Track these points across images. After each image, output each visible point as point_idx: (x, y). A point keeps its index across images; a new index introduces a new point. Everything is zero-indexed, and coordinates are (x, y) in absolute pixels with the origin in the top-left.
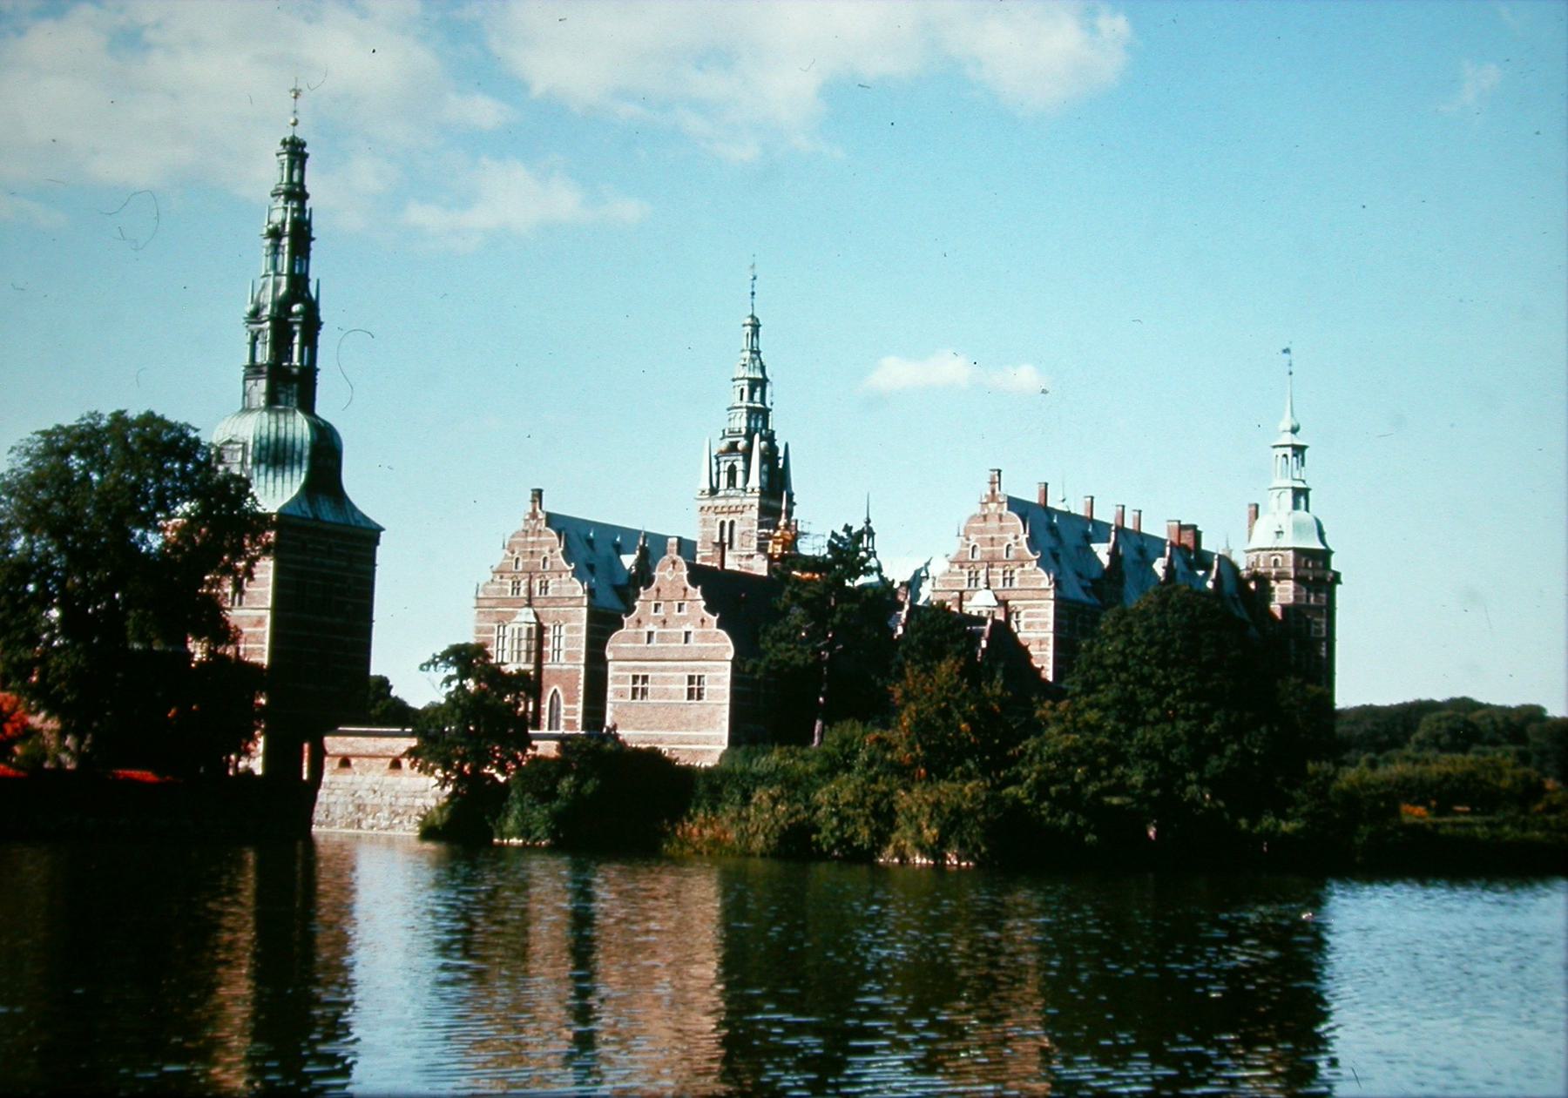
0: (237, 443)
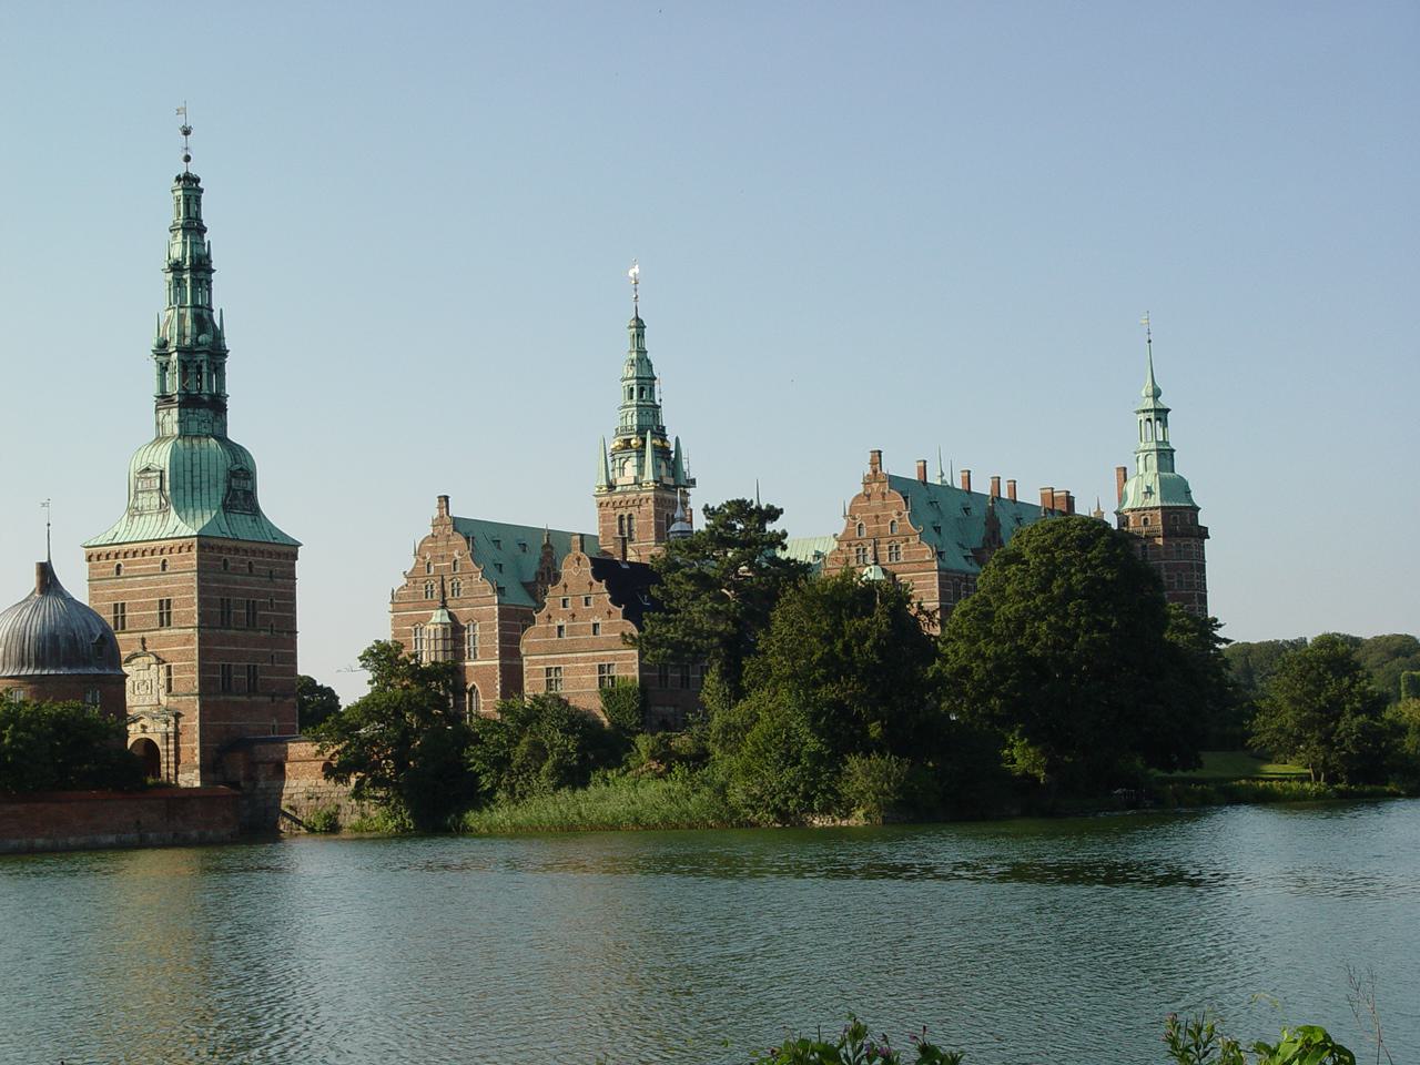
0: (155, 471)
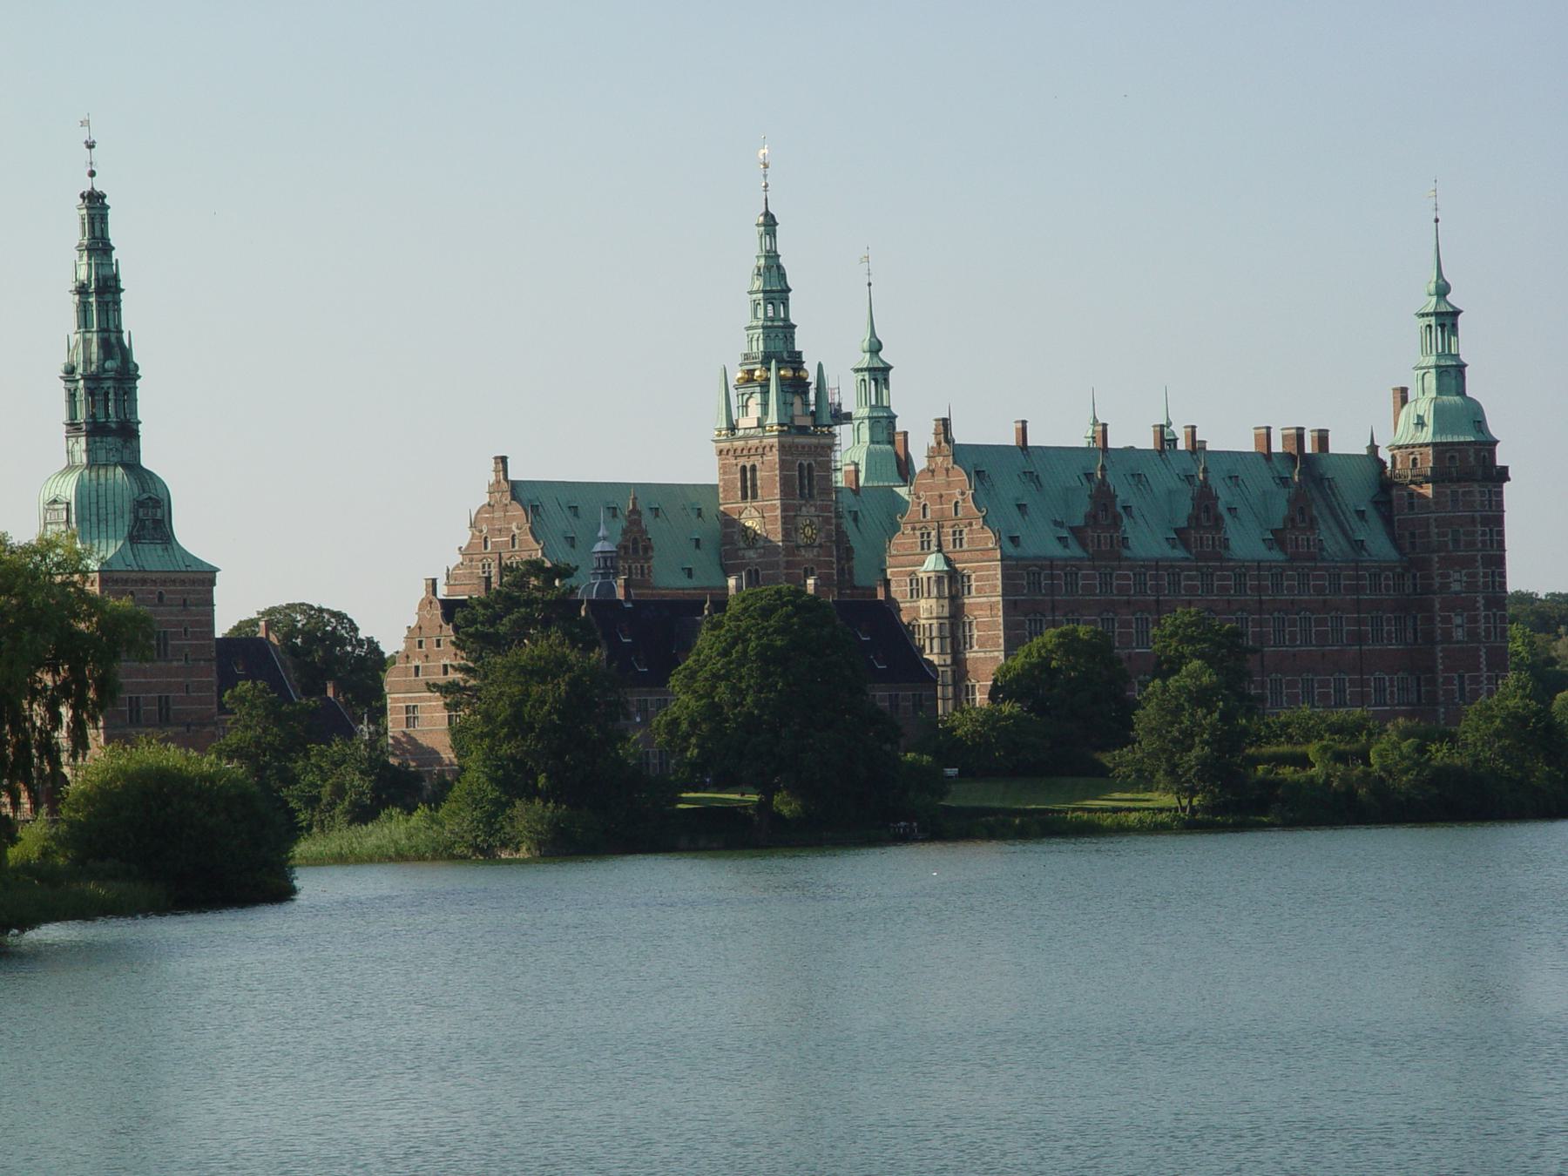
0: (62, 504)
